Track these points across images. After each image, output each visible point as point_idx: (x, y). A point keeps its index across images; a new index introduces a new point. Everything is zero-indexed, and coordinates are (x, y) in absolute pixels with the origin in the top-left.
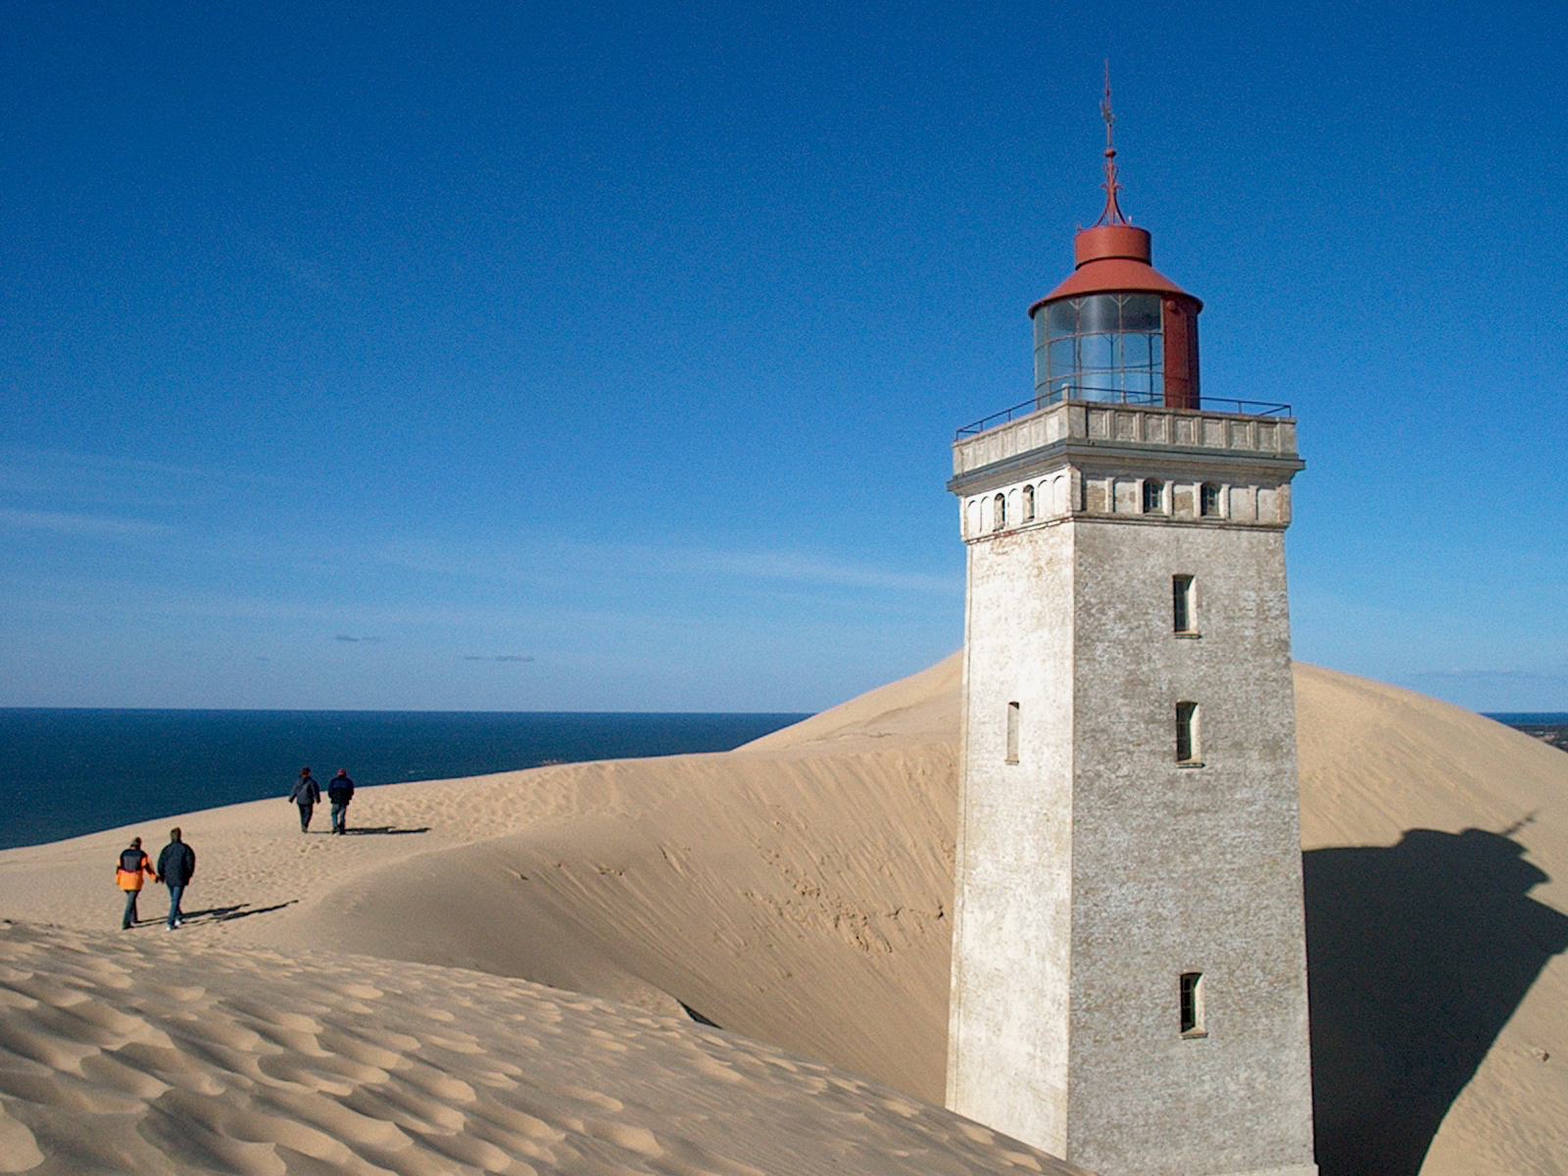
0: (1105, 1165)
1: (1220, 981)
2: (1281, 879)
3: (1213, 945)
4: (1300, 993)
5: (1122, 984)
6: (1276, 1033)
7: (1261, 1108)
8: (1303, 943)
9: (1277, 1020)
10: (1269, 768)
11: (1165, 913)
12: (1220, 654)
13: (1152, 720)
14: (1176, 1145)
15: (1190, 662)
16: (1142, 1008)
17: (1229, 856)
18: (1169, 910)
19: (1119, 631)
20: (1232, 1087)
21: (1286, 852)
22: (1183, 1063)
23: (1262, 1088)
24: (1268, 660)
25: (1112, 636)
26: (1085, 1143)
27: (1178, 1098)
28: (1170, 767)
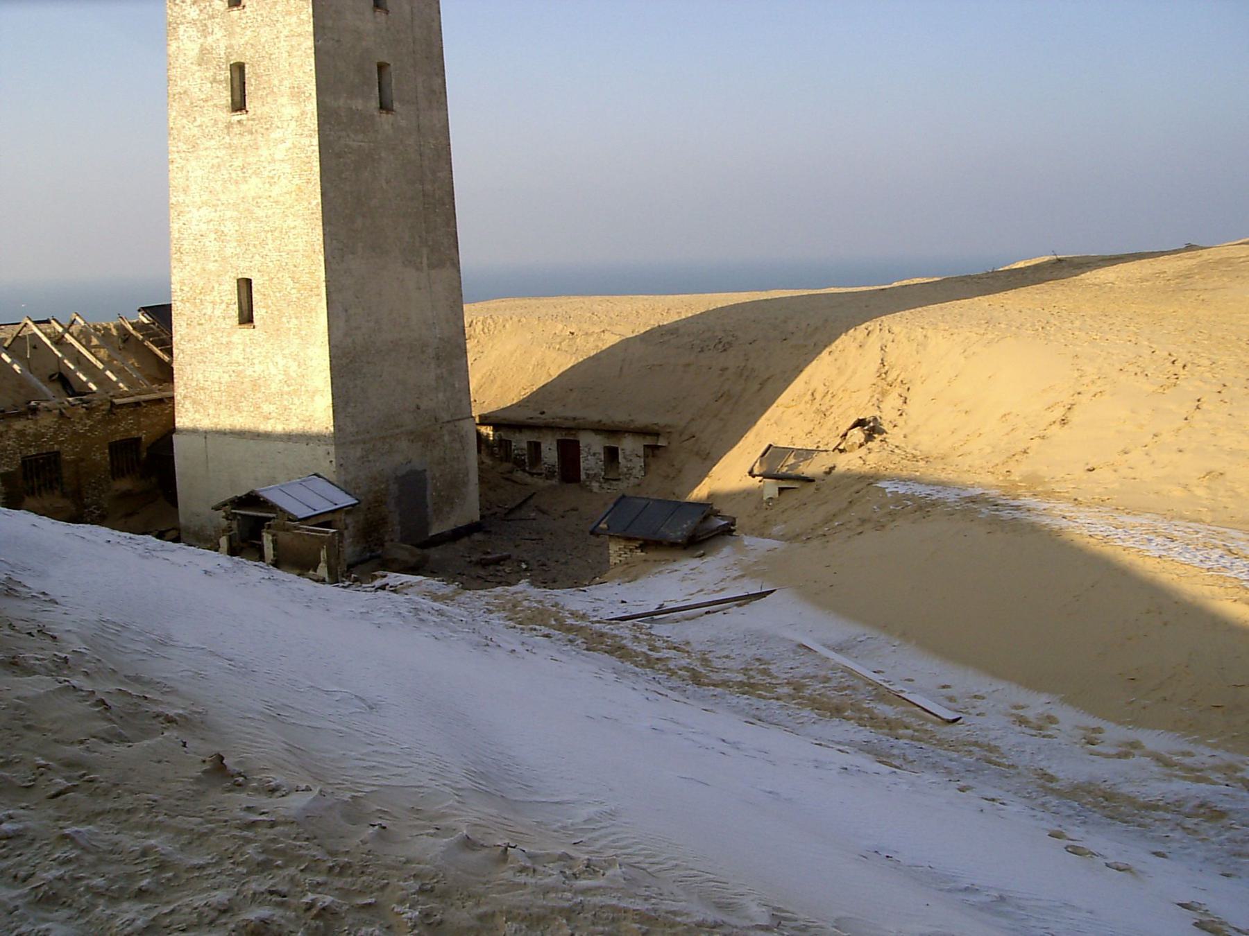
0: (197, 416)
1: (263, 285)
2: (306, 204)
3: (257, 257)
4: (320, 301)
5: (201, 284)
6: (303, 333)
7: (295, 391)
8: (322, 258)
9: (304, 320)
10: (295, 112)
11: (226, 231)
12: (260, 18)
13: (214, 81)
14: (239, 409)
15: (238, 30)
16: (214, 303)
17: (267, 185)
18: (230, 228)
19: (193, 12)
20: (273, 371)
21: (308, 182)
22: (241, 347)
23: (294, 375)
24: (294, 19)
25: (189, 18)
26: (185, 397)
27: (238, 374)
28: (226, 116)
